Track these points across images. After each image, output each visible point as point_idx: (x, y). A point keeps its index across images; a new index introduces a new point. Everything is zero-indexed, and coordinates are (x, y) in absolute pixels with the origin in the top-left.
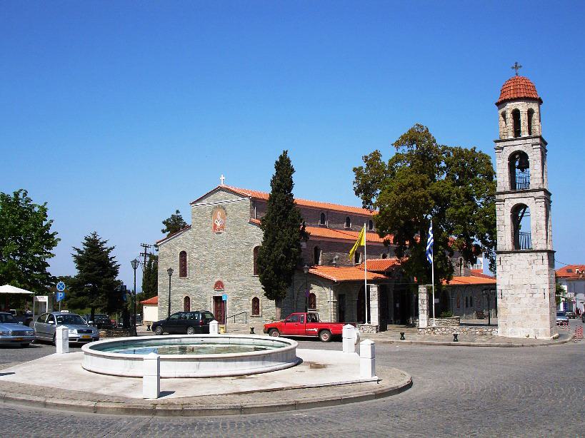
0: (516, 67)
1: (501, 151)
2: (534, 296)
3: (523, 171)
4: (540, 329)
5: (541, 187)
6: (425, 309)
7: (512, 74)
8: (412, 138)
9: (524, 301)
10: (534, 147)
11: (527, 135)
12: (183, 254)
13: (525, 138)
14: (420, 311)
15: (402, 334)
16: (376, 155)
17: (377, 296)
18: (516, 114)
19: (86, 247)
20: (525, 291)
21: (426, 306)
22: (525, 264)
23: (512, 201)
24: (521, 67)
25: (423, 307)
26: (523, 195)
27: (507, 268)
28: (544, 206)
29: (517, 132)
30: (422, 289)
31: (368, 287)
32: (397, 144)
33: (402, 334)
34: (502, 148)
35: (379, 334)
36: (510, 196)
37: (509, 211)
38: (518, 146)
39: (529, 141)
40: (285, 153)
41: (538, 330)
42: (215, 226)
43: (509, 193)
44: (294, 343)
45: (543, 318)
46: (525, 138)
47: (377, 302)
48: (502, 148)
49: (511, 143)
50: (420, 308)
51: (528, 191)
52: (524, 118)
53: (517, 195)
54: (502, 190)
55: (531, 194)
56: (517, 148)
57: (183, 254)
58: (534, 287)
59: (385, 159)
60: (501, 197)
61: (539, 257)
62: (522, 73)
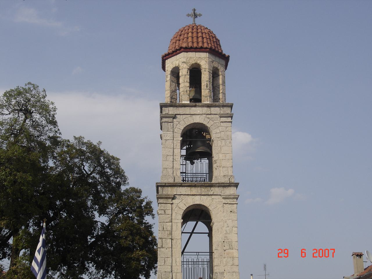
0: (195, 16)
1: (170, 120)
3: (192, 163)
5: (233, 181)
7: (190, 21)
24: (200, 15)
26: (204, 190)
29: (196, 100)
34: (174, 117)
43: (181, 185)
46: (208, 106)
48: (174, 117)
49: (187, 110)
51: (211, 186)
52: (205, 77)
53: (194, 191)
55: (216, 190)
56: (197, 120)
62: (199, 21)
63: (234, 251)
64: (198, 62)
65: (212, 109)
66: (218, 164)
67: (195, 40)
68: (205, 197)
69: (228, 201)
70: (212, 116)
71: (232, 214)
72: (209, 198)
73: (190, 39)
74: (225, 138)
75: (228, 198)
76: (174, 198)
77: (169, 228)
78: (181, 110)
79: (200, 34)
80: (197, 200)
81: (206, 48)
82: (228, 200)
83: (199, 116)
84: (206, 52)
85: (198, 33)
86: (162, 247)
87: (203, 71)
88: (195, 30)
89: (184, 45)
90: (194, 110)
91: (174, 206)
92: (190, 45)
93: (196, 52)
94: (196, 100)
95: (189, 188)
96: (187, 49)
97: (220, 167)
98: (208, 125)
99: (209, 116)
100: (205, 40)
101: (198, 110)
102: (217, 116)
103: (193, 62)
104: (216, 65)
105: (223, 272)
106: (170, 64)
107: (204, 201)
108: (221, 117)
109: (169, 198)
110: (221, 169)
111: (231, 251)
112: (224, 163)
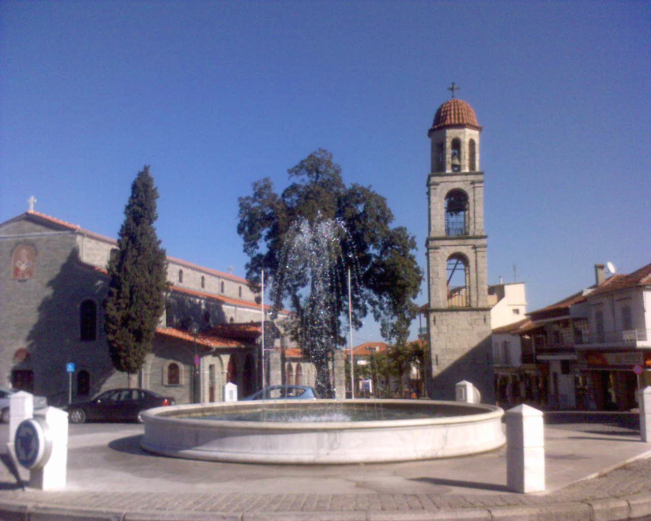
8: (312, 165)
11: (467, 170)
13: (466, 174)
19: (410, 238)
24: (458, 88)
26: (462, 242)
27: (444, 328)
29: (457, 169)
32: (295, 171)
40: (146, 169)
42: (17, 270)
52: (465, 149)
53: (455, 242)
54: (438, 235)
56: (457, 185)
59: (278, 190)
60: (437, 243)
98: (466, 190)
101: (458, 178)
103: (454, 136)
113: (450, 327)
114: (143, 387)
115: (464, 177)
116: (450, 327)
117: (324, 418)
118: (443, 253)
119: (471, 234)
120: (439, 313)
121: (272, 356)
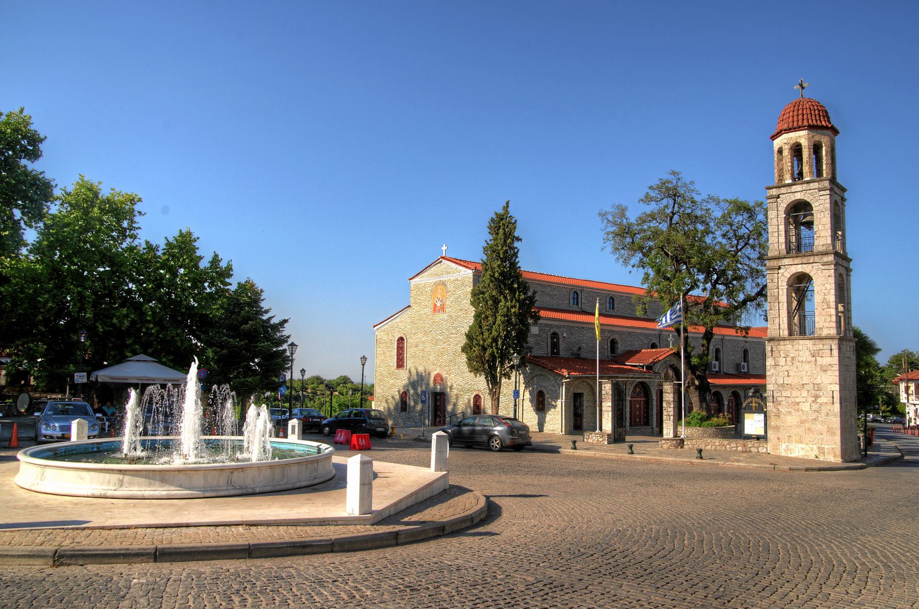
2: (819, 400)
4: (826, 447)
6: (671, 413)
9: (806, 407)
10: (822, 193)
12: (401, 340)
13: (808, 182)
14: (664, 417)
15: (574, 442)
16: (622, 211)
17: (610, 397)
18: (797, 150)
20: (805, 394)
21: (672, 409)
22: (805, 355)
23: (791, 268)
25: (669, 411)
27: (782, 361)
28: (833, 275)
29: (798, 177)
30: (668, 388)
31: (600, 383)
32: (648, 199)
33: (574, 442)
35: (612, 445)
36: (786, 261)
37: (785, 284)
38: (799, 193)
39: (816, 185)
41: (824, 448)
42: (435, 305)
44: (319, 444)
45: (830, 431)
46: (808, 182)
47: (610, 404)
50: (665, 413)
55: (817, 259)
56: (798, 196)
57: (401, 340)
58: (818, 387)
59: (632, 216)
61: (825, 347)
63: (831, 310)
64: (798, 141)
65: (811, 184)
66: (818, 235)
67: (795, 118)
68: (806, 265)
69: (826, 267)
70: (812, 191)
71: (830, 278)
72: (810, 266)
73: (791, 119)
74: (824, 210)
75: (826, 265)
76: (779, 268)
77: (776, 294)
78: (783, 190)
79: (800, 112)
80: (800, 269)
81: (804, 126)
82: (826, 266)
83: (799, 193)
84: (805, 130)
85: (798, 110)
86: (771, 309)
87: (803, 147)
88: (796, 108)
89: (785, 127)
90: (794, 188)
91: (780, 275)
92: (791, 126)
93: (795, 131)
94: (798, 177)
95: (792, 259)
96: (789, 130)
97: (820, 237)
99: (809, 192)
100: (805, 117)
102: (816, 190)
103: (792, 142)
104: (817, 138)
105: (822, 328)
106: (778, 143)
107: (806, 269)
108: (820, 191)
109: (775, 269)
110: (820, 238)
111: (829, 310)
112: (822, 234)
113: (789, 359)
114: (500, 414)
115: (805, 186)
116: (789, 359)
117: (572, 454)
118: (783, 275)
119: (815, 251)
120: (777, 343)
121: (605, 387)
